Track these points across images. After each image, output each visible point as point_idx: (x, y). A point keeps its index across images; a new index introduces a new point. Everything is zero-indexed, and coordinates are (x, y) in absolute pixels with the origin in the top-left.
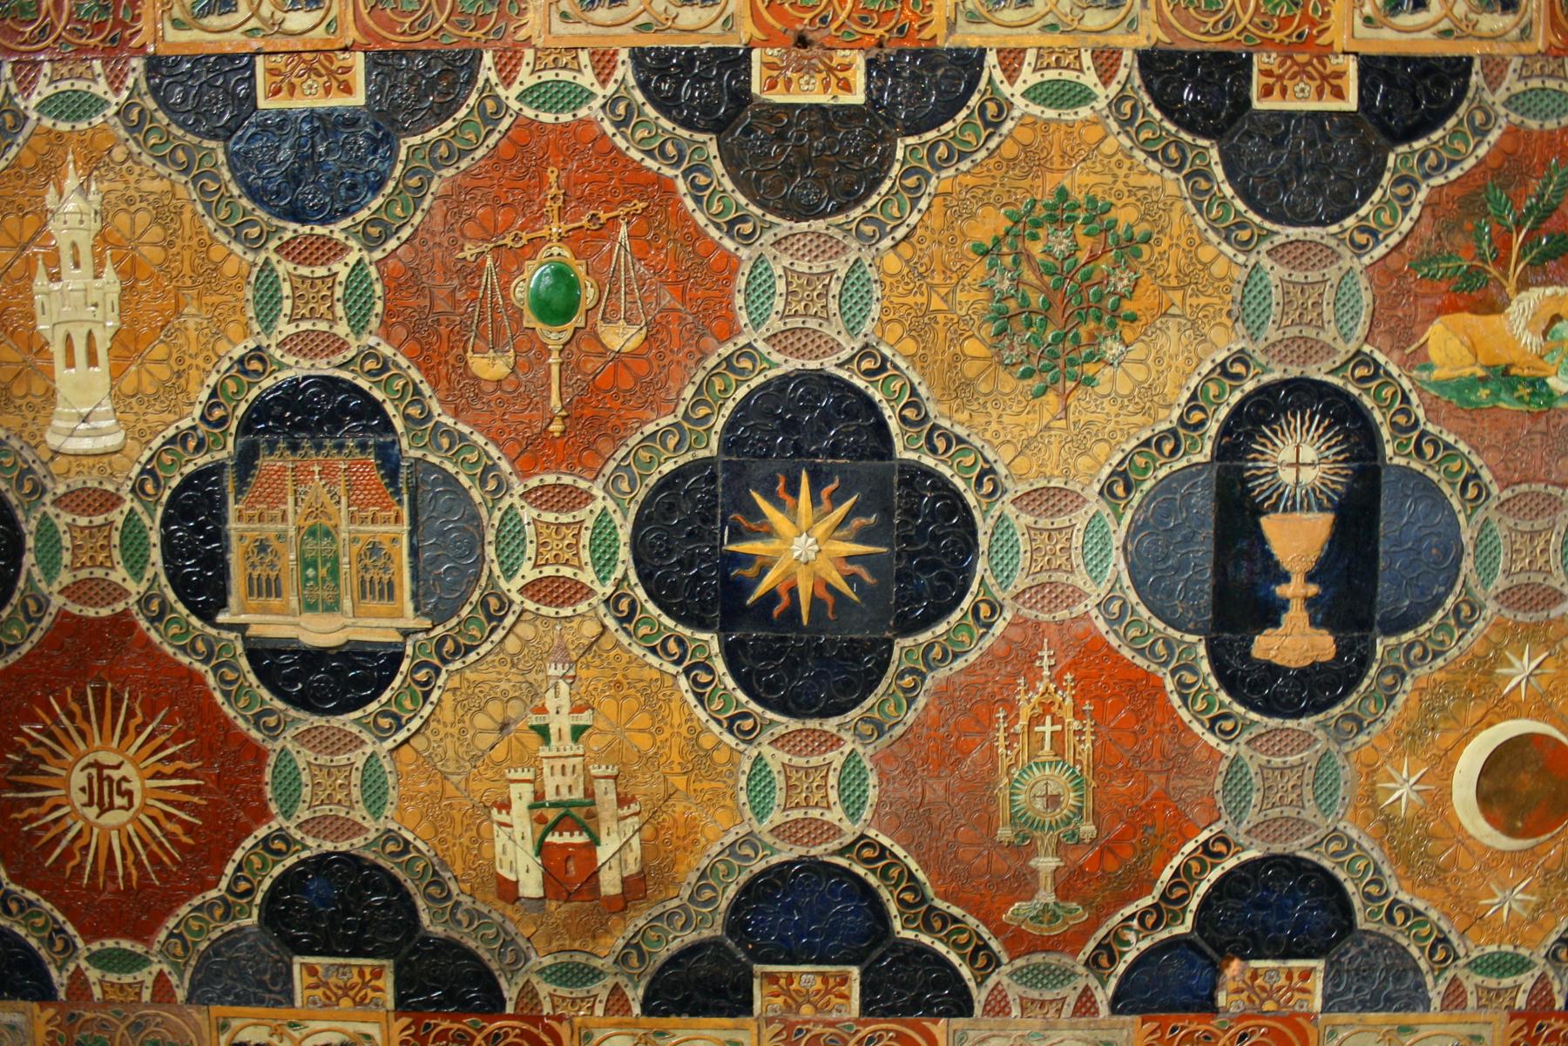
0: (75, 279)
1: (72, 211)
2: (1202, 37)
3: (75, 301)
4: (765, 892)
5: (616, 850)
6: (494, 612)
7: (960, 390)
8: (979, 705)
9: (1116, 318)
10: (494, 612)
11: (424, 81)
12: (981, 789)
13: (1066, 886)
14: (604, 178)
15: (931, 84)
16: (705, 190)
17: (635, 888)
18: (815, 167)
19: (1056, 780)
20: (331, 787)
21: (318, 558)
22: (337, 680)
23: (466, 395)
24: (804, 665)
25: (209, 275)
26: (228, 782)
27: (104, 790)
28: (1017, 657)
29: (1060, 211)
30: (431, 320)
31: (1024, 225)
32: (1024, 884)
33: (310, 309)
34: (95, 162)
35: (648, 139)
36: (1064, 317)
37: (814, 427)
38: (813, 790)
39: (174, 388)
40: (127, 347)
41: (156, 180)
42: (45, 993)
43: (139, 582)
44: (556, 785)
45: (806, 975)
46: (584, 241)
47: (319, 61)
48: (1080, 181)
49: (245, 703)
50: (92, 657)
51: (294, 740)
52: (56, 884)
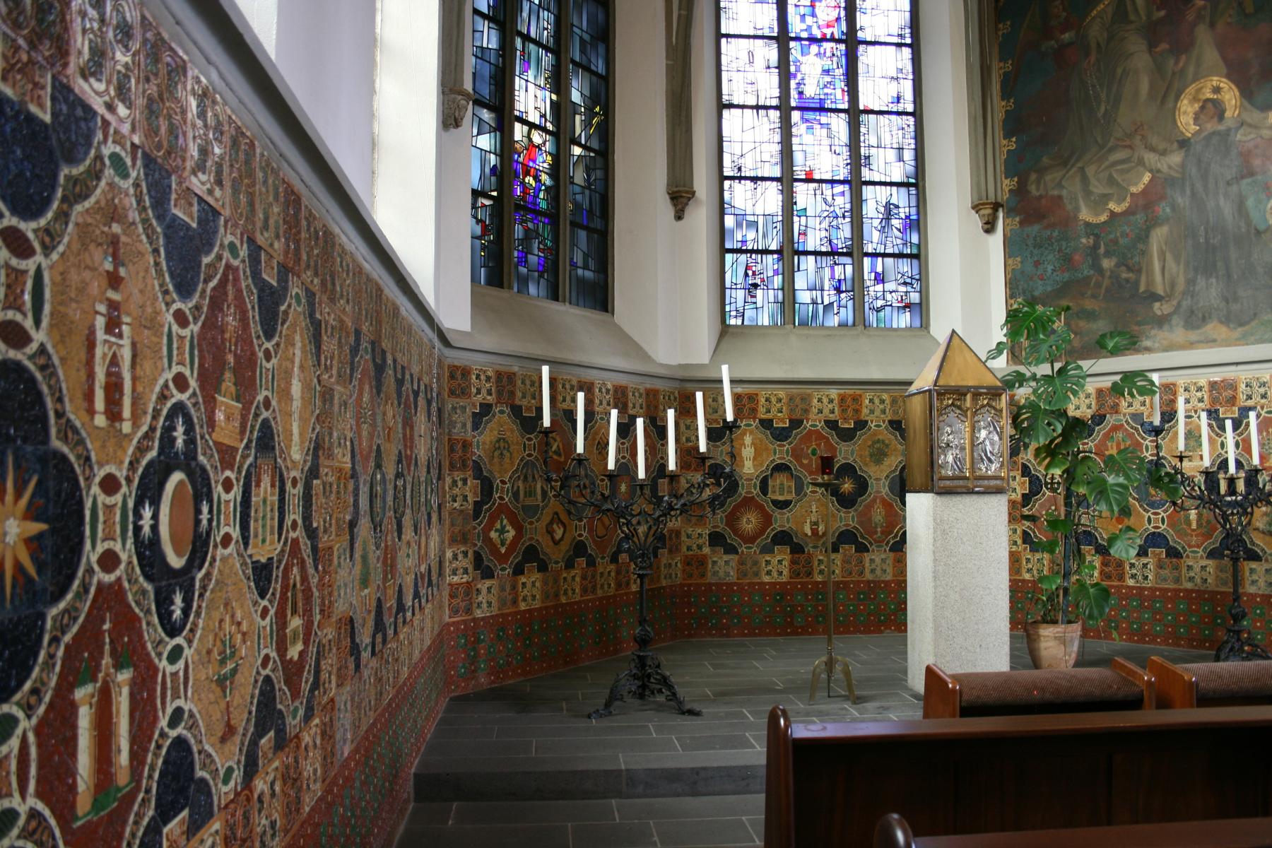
0: (748, 449)
1: (748, 439)
2: (896, 418)
3: (748, 452)
4: (841, 534)
5: (821, 529)
6: (805, 495)
7: (866, 465)
8: (870, 507)
9: (886, 455)
10: (805, 495)
11: (796, 423)
12: (870, 520)
13: (882, 533)
14: (820, 436)
15: (861, 425)
16: (833, 439)
17: (824, 534)
18: (847, 435)
19: (879, 517)
20: (782, 521)
21: (781, 488)
22: (784, 505)
23: (802, 465)
24: (847, 502)
25: (767, 449)
26: (767, 520)
27: (749, 522)
28: (874, 501)
29: (878, 441)
30: (797, 454)
31: (874, 443)
32: (876, 532)
33: (781, 453)
34: (751, 433)
35: (826, 432)
36: (879, 455)
37: (848, 470)
38: (848, 519)
39: (762, 465)
40: (755, 459)
41: (760, 436)
42: (737, 553)
43: (756, 491)
44: (814, 519)
45: (847, 546)
46: (818, 445)
47: (782, 420)
48: (881, 437)
49: (770, 508)
50: (748, 502)
51: (777, 514)
52: (741, 536)
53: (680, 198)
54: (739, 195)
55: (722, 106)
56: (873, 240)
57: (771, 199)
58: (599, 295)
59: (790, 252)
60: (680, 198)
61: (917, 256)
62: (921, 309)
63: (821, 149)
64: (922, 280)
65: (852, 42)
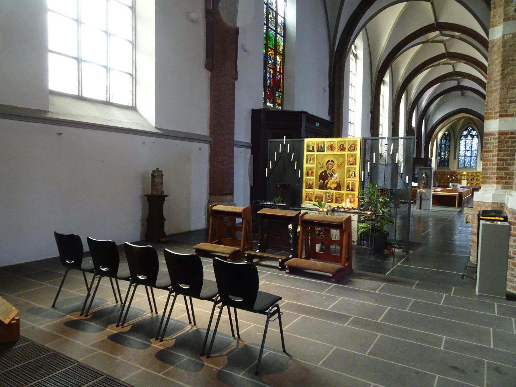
53: (455, 159)
54: (460, 158)
55: (460, 151)
56: (472, 161)
57: (464, 158)
58: (448, 166)
59: (465, 162)
60: (455, 159)
61: (476, 162)
62: (476, 166)
63: (468, 154)
64: (476, 164)
65: (472, 145)
